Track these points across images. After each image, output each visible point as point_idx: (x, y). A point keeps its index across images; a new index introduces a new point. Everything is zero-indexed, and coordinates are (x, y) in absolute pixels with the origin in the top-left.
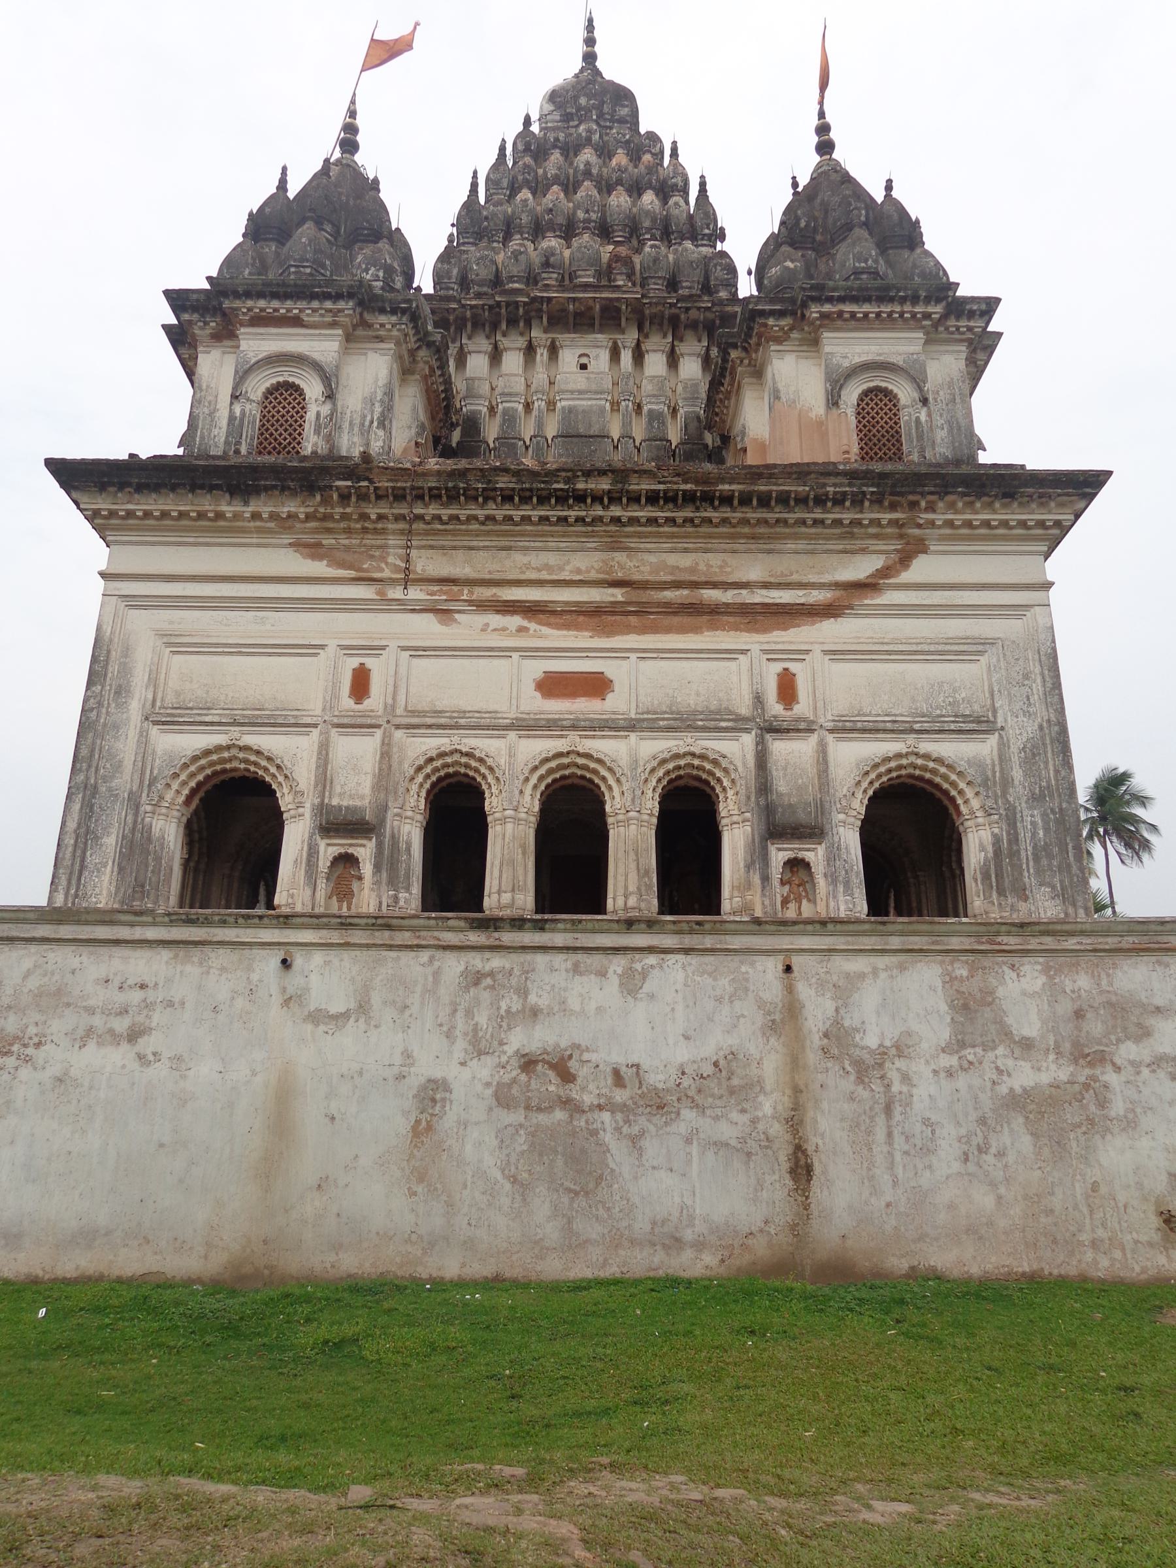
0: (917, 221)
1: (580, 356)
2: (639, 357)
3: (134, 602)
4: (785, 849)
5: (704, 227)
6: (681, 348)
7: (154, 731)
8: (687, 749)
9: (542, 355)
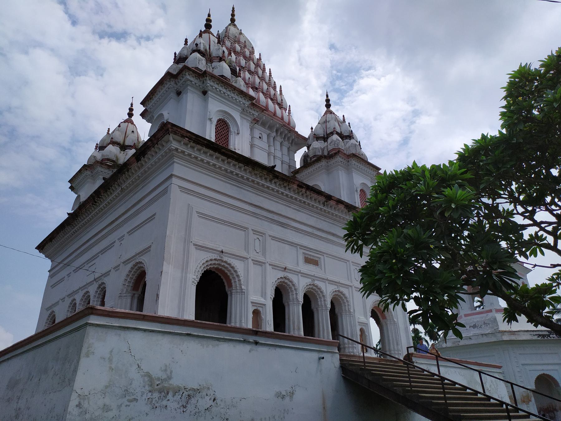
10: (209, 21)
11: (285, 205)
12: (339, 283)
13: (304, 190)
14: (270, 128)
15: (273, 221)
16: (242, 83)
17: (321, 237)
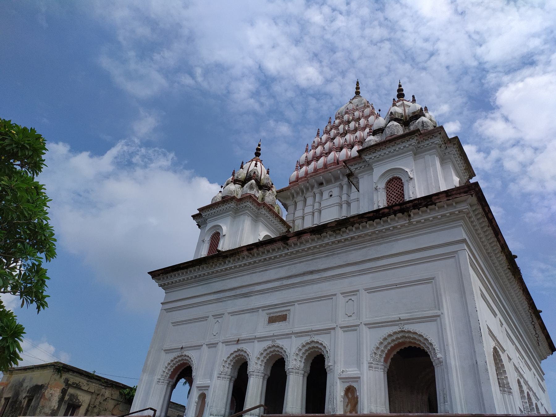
3: (168, 310)
9: (318, 196)
10: (258, 149)
11: (251, 273)
12: (312, 331)
13: (255, 250)
14: (337, 179)
15: (236, 297)
16: (371, 137)
17: (293, 284)
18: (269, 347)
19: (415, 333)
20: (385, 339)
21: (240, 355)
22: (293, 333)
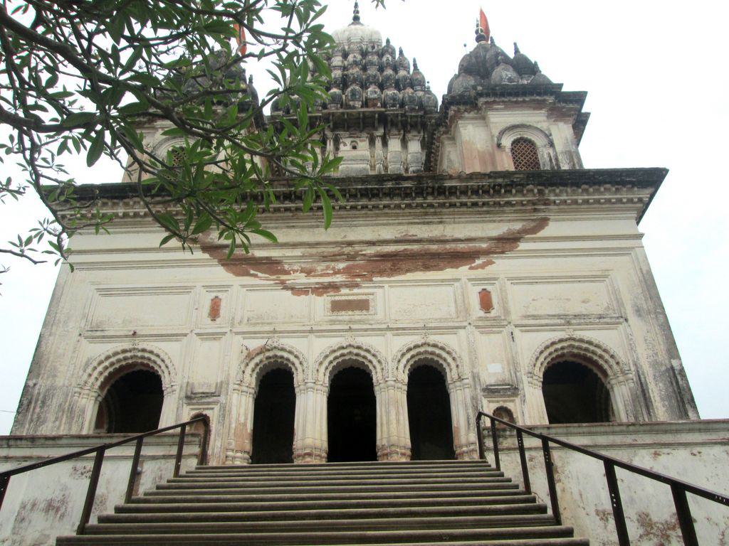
0: (536, 63)
1: (352, 142)
2: (385, 144)
4: (493, 402)
5: (416, 82)
6: (409, 136)
7: (84, 341)
8: (423, 341)
18: (343, 348)
19: (590, 343)
20: (547, 347)
21: (276, 356)
22: (389, 329)
